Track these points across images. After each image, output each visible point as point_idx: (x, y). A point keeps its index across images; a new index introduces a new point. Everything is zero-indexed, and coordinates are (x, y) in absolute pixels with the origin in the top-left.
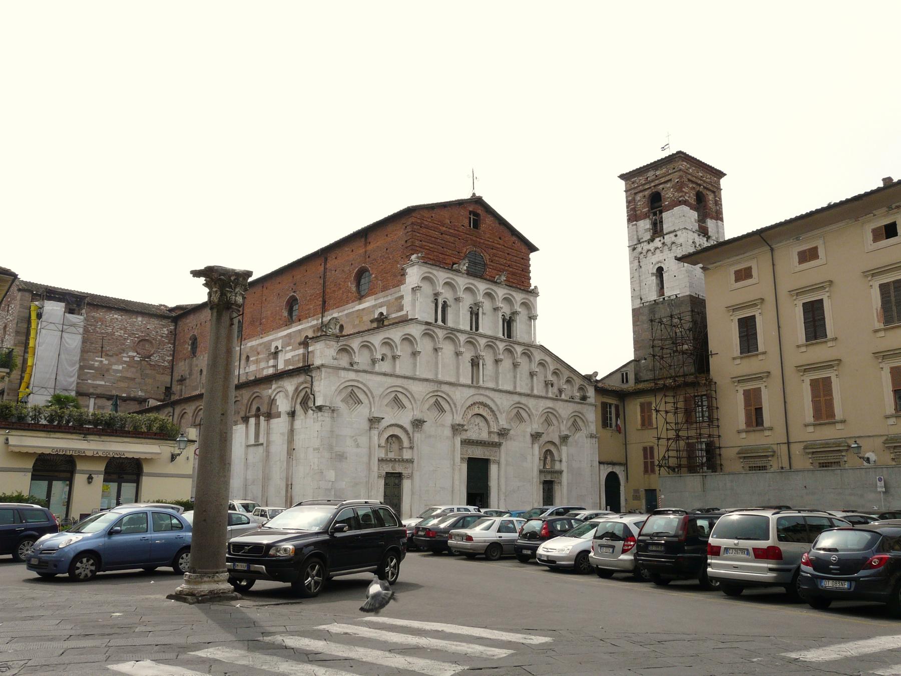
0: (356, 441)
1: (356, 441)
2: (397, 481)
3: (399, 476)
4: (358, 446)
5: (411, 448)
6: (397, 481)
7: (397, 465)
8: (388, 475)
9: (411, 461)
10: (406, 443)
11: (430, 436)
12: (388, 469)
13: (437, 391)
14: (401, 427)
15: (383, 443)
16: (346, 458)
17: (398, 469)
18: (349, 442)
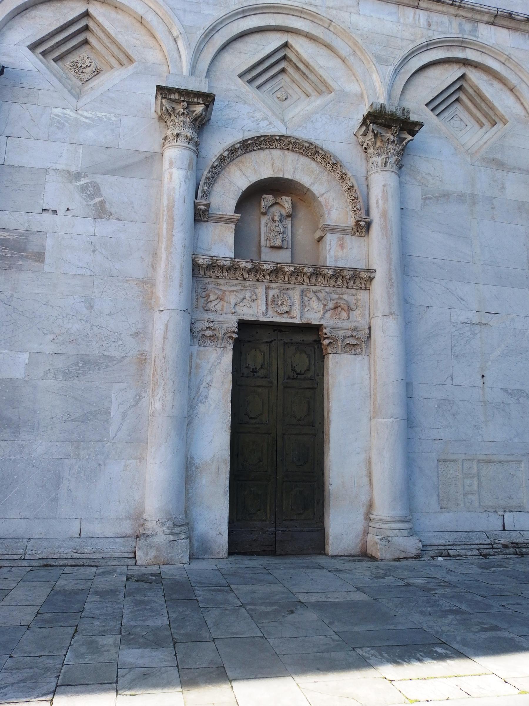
0: (92, 191)
1: (92, 191)
2: (301, 361)
3: (309, 341)
4: (101, 212)
5: (363, 227)
6: (301, 361)
7: (295, 295)
8: (248, 335)
9: (358, 278)
10: (337, 210)
11: (445, 196)
12: (256, 305)
13: (462, 44)
14: (310, 150)
15: (225, 197)
16: (40, 257)
17: (306, 307)
18: (55, 192)
